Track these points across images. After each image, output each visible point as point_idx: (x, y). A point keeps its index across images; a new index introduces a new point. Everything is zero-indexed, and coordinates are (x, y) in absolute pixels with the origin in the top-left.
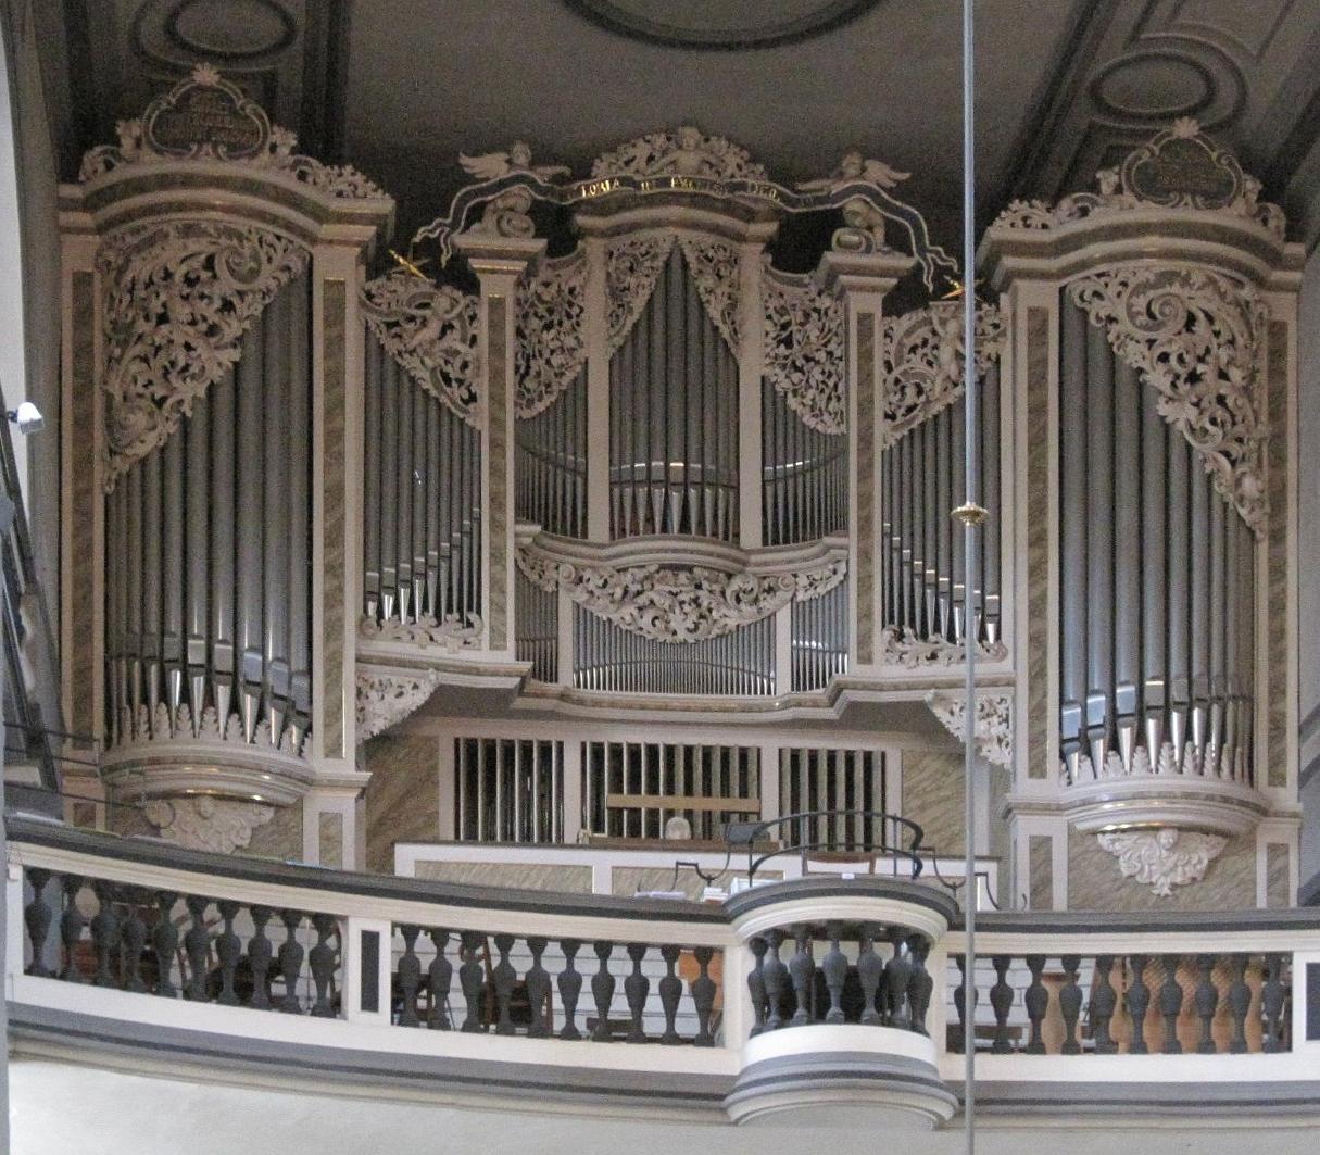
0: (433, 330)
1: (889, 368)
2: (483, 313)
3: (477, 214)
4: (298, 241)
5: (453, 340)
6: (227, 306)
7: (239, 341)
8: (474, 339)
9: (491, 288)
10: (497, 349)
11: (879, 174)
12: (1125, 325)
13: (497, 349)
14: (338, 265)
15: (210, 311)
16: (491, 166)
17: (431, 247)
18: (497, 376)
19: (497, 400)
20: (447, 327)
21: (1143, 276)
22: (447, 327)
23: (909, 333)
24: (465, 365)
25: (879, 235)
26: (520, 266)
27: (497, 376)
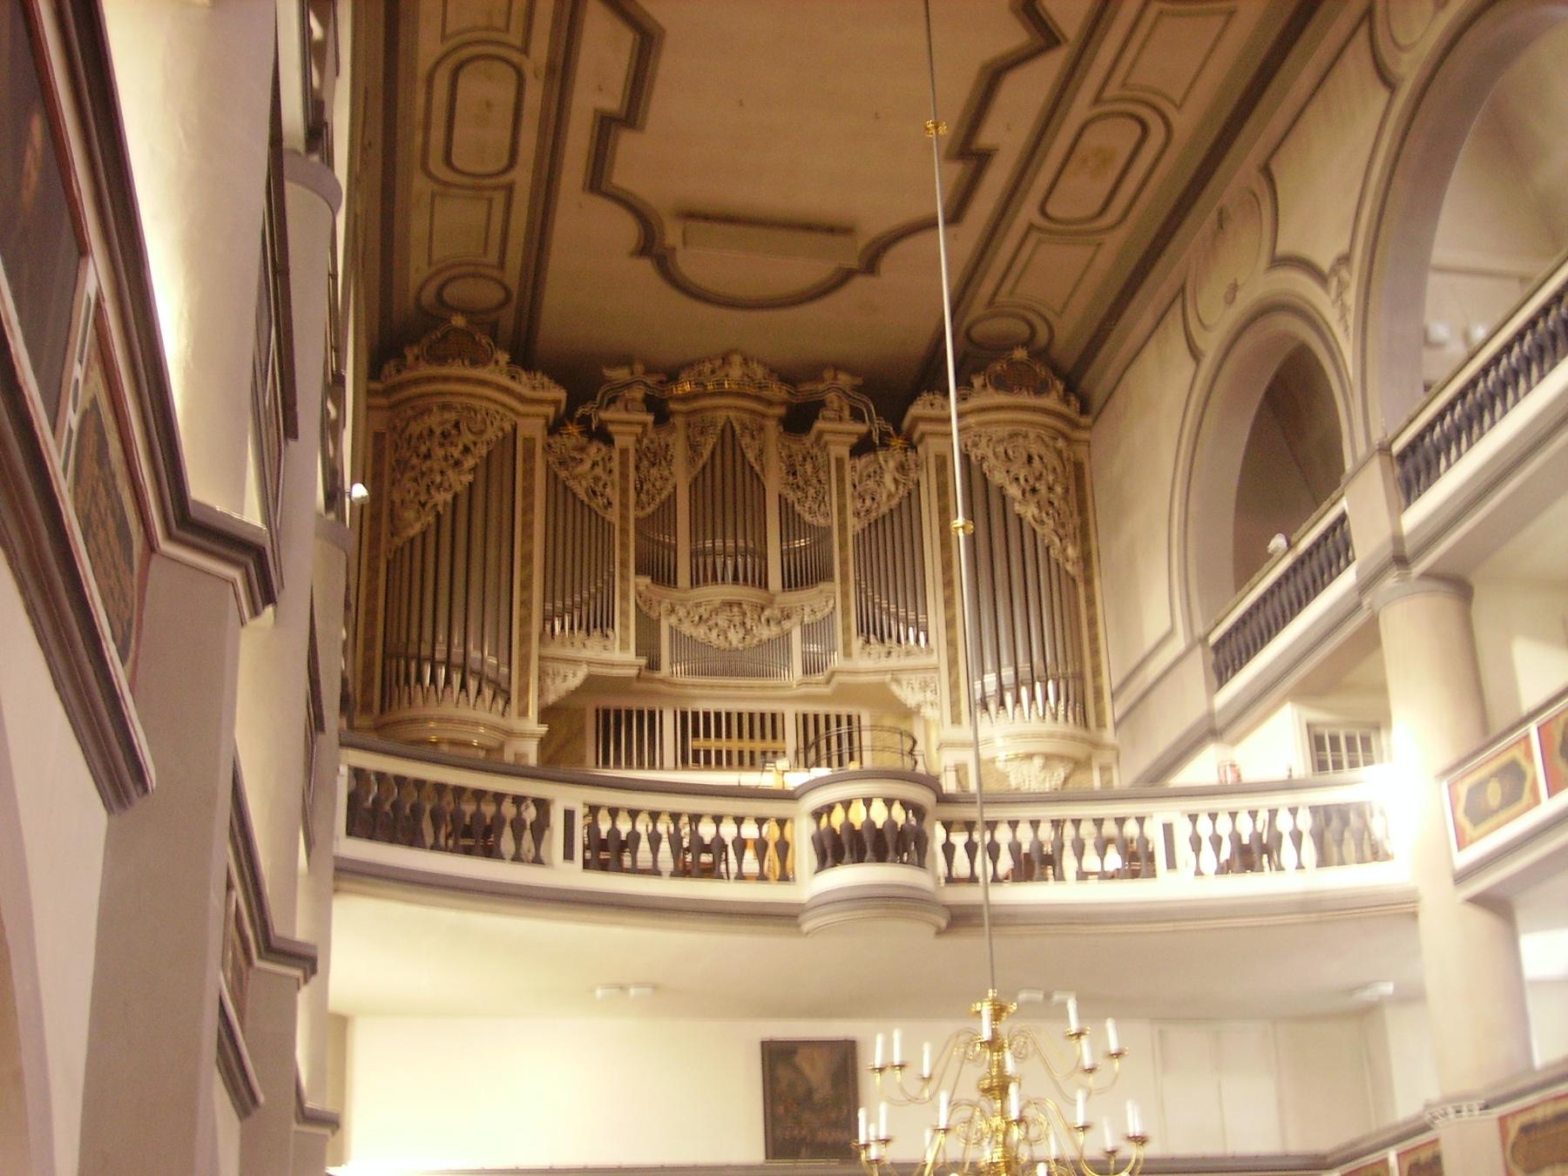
0: (588, 464)
3: (612, 401)
4: (509, 414)
5: (599, 471)
6: (466, 450)
7: (474, 470)
9: (619, 441)
10: (624, 476)
11: (844, 379)
13: (624, 476)
15: (456, 453)
16: (620, 374)
17: (585, 420)
18: (624, 492)
19: (624, 506)
20: (595, 464)
23: (866, 467)
24: (605, 486)
25: (846, 413)
27: (624, 492)
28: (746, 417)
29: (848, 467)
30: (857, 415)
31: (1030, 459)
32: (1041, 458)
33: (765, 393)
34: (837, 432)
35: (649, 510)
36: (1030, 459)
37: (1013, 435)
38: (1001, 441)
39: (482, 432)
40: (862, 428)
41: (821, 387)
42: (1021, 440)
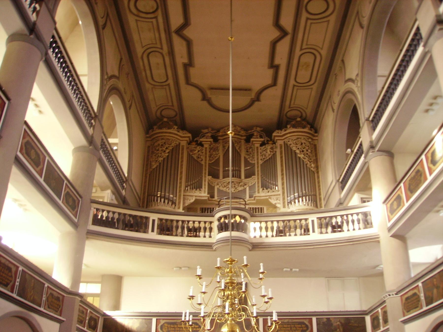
0: (197, 151)
1: (261, 153)
2: (204, 149)
3: (203, 137)
5: (199, 153)
6: (167, 148)
8: (203, 153)
11: (258, 129)
12: (292, 145)
13: (206, 154)
14: (184, 143)
16: (206, 131)
17: (197, 141)
19: (206, 160)
20: (199, 151)
21: (295, 138)
22: (199, 151)
25: (258, 136)
26: (209, 143)
27: (206, 157)
28: (236, 139)
29: (259, 148)
30: (261, 137)
31: (302, 144)
32: (305, 143)
33: (240, 133)
34: (256, 141)
35: (213, 161)
36: (302, 144)
37: (298, 138)
38: (295, 140)
39: (171, 144)
40: (262, 140)
41: (253, 131)
42: (299, 140)
